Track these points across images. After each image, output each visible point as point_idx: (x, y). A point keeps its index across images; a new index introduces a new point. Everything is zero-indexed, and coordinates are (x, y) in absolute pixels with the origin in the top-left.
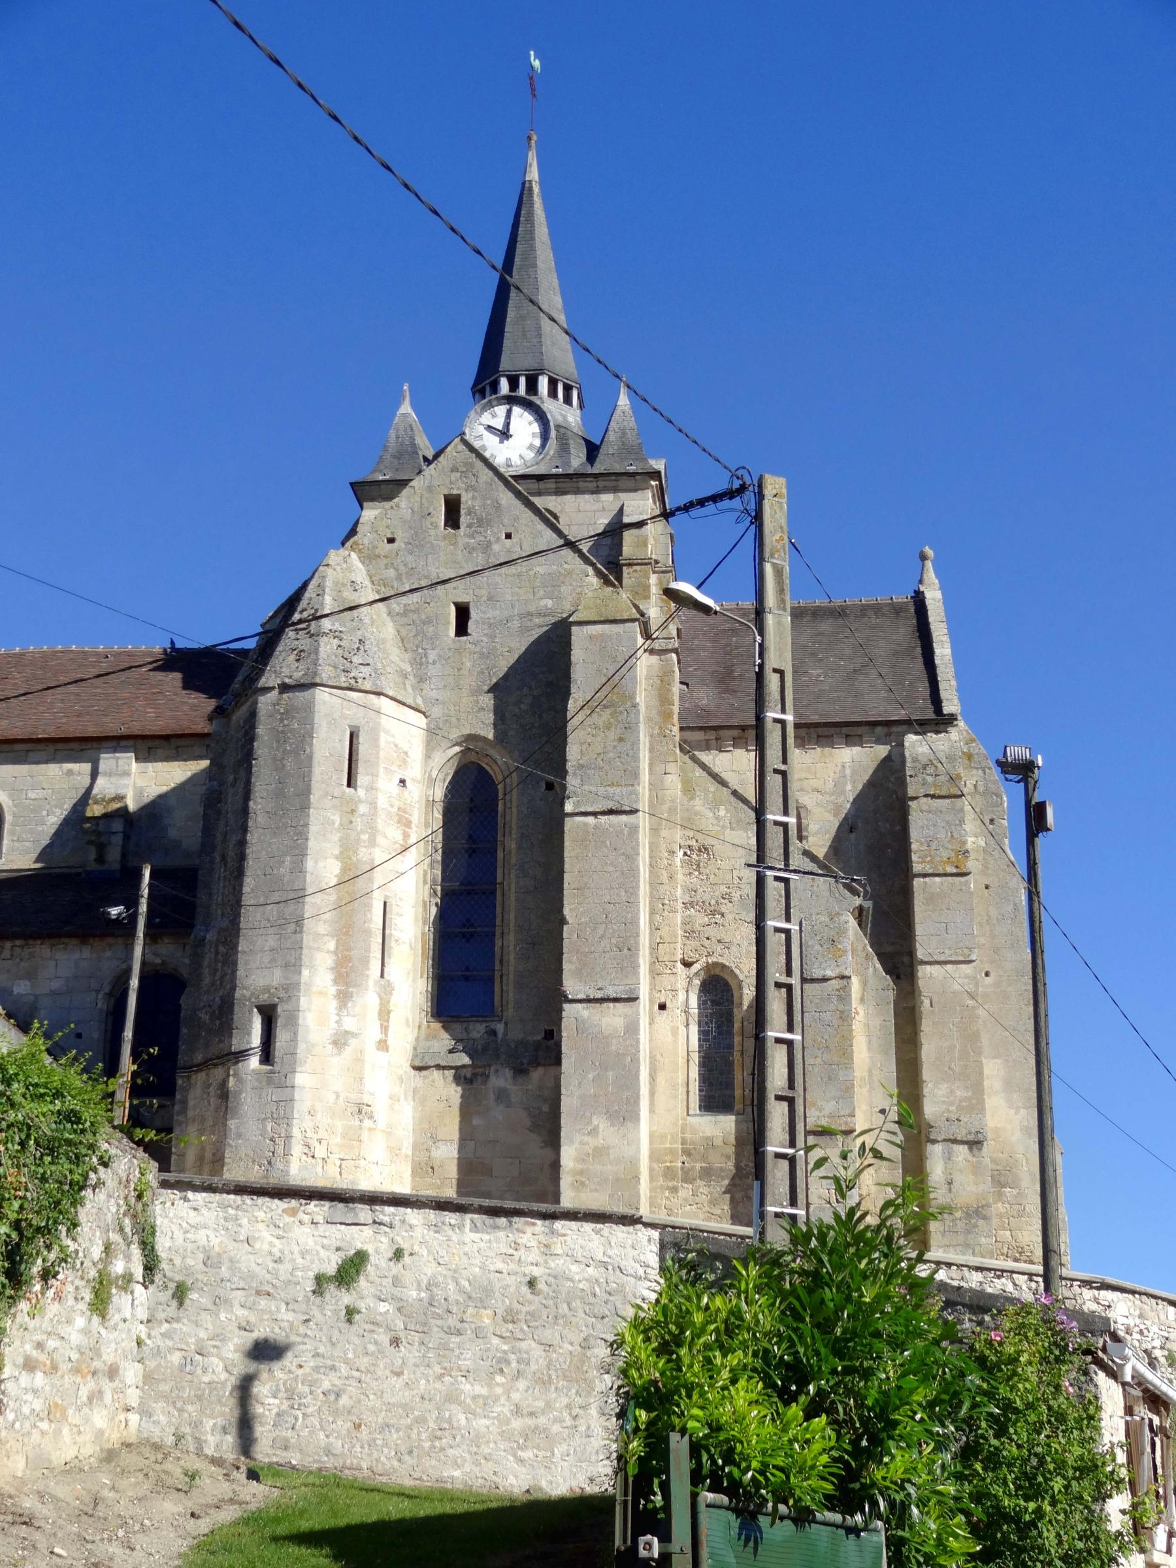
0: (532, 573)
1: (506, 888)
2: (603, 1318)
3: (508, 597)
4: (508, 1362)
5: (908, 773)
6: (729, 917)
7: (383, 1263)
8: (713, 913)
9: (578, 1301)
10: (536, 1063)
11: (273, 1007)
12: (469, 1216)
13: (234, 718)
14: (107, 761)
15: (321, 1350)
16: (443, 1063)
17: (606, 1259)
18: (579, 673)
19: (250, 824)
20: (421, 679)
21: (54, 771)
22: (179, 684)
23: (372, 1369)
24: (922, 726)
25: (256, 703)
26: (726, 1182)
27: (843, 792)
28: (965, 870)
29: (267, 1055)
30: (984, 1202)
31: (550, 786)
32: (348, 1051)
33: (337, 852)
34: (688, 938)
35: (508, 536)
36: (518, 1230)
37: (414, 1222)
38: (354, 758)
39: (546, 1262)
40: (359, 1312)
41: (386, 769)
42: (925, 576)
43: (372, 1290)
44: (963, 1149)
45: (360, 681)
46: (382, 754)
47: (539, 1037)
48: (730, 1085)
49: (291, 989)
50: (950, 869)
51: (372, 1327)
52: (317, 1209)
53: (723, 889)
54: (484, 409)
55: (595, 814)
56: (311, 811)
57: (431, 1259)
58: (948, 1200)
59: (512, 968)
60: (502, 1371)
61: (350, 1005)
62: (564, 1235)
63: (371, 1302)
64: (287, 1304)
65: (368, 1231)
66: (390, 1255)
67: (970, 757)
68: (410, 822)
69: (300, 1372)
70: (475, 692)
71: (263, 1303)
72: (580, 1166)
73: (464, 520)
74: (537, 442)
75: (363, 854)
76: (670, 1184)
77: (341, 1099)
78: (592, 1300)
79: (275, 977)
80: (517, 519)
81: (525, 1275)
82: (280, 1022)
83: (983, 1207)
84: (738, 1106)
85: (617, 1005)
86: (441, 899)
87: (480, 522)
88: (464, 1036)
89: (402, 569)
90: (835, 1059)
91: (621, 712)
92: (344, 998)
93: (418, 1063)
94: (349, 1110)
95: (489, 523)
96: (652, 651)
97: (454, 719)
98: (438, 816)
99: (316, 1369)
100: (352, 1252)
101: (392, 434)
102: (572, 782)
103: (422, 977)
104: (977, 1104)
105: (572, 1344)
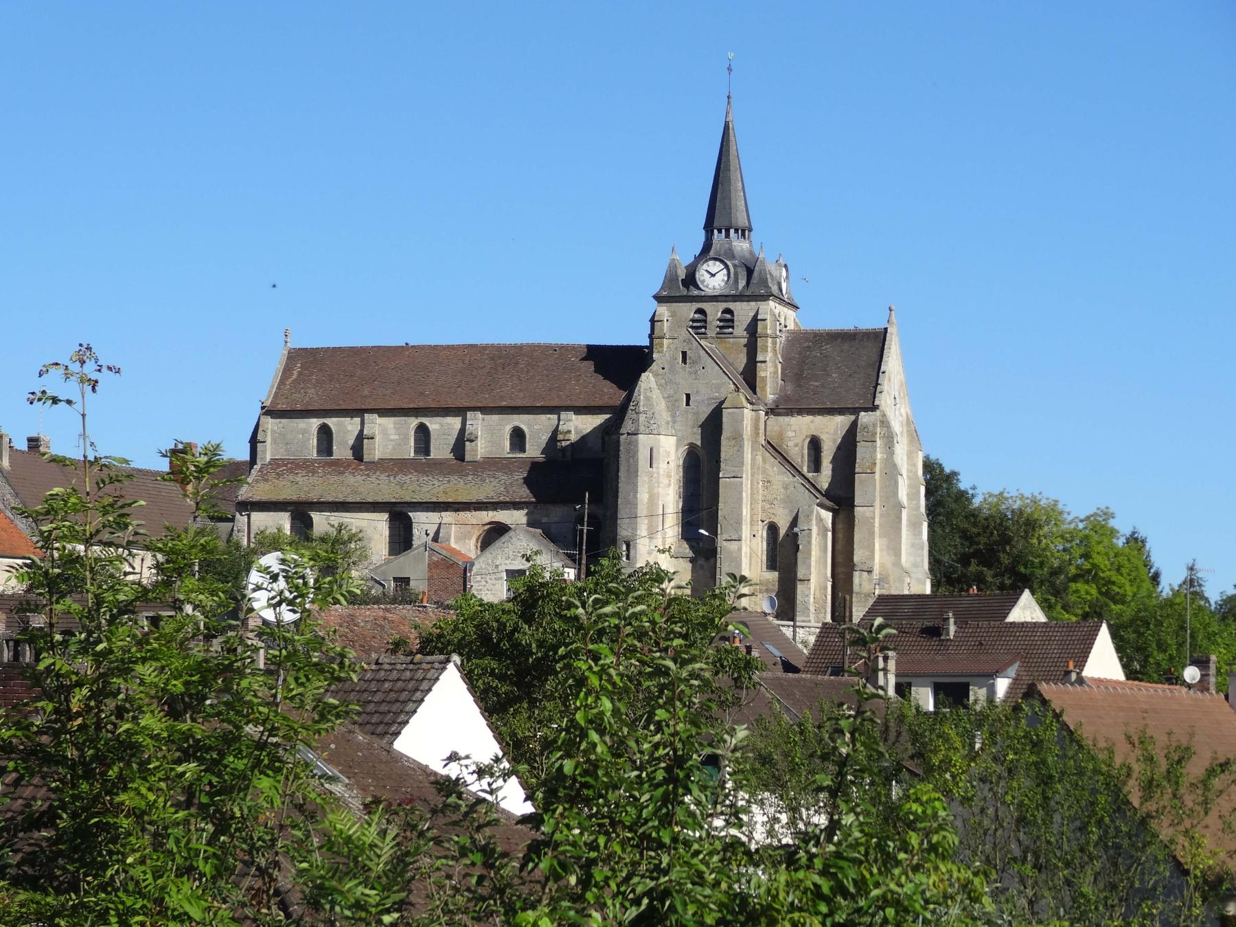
14: (563, 415)
18: (725, 426)
21: (543, 417)
24: (866, 410)
70: (693, 427)
74: (726, 278)
75: (656, 491)
98: (681, 470)
102: (722, 465)
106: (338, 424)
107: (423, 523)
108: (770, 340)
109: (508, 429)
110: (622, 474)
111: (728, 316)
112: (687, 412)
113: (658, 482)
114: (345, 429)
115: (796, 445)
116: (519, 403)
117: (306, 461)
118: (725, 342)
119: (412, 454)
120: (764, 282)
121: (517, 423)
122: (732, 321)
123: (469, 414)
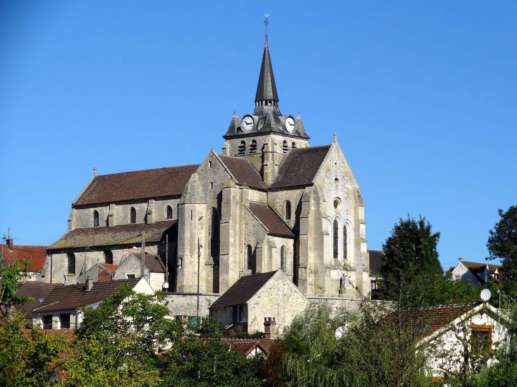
18: (223, 197)
44: (304, 269)
46: (196, 214)
49: (183, 255)
55: (224, 223)
70: (214, 199)
75: (194, 232)
92: (191, 256)
98: (210, 221)
102: (222, 217)
106: (101, 210)
107: (118, 255)
108: (270, 154)
109: (165, 206)
111: (254, 144)
112: (211, 191)
113: (195, 227)
114: (103, 211)
115: (280, 206)
116: (169, 194)
117: (89, 229)
118: (253, 157)
119: (129, 222)
120: (269, 125)
121: (168, 204)
122: (256, 146)
123: (150, 201)
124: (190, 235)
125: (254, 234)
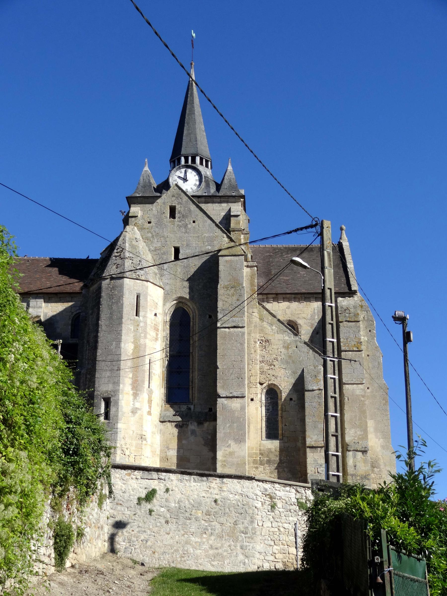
0: (203, 236)
1: (194, 354)
2: (241, 514)
3: (194, 245)
4: (208, 530)
5: (339, 312)
6: (277, 366)
7: (162, 493)
8: (271, 365)
9: (232, 508)
10: (206, 420)
11: (109, 398)
12: (193, 476)
13: (91, 289)
14: (33, 302)
15: (140, 525)
16: (171, 420)
17: (242, 493)
18: (222, 274)
19: (99, 329)
20: (162, 275)
22: (57, 272)
23: (159, 532)
25: (101, 284)
26: (276, 465)
27: (314, 319)
28: (361, 349)
29: (107, 416)
30: (368, 474)
31: (210, 317)
32: (137, 415)
33: (132, 341)
34: (261, 374)
35: (194, 222)
36: (210, 482)
37: (173, 478)
38: (138, 305)
39: (220, 493)
40: (154, 511)
41: (150, 309)
42: (342, 236)
43: (158, 503)
44: (360, 454)
45: (140, 276)
46: (149, 304)
47: (207, 410)
48: (277, 429)
49: (116, 392)
50: (355, 349)
51: (158, 517)
52: (138, 474)
53: (275, 356)
54: (177, 170)
55: (229, 328)
56: (123, 325)
57: (179, 492)
58: (355, 473)
59: (196, 385)
60: (205, 533)
61: (138, 398)
62: (227, 484)
63: (158, 508)
64: (128, 508)
65: (156, 482)
66: (165, 490)
67: (362, 306)
68: (158, 329)
69: (133, 533)
71: (119, 508)
72: (224, 459)
73: (177, 215)
74: (198, 183)
75: (142, 341)
76: (255, 466)
77: (135, 433)
78: (237, 507)
79: (110, 387)
80: (197, 215)
81: (213, 498)
82: (112, 404)
83: (367, 475)
84: (280, 437)
85: (238, 399)
86: (169, 358)
87: (183, 216)
88: (179, 410)
89: (154, 233)
90: (317, 420)
91: (238, 290)
92: (135, 395)
93: (162, 420)
94: (138, 437)
95: (187, 217)
96: (248, 266)
97: (174, 291)
98: (168, 327)
99: (139, 532)
100: (151, 489)
101: (141, 178)
103: (162, 387)
104: (365, 437)
105: (230, 523)
110: (103, 322)
113: (145, 332)
124: (133, 348)
125: (287, 363)
